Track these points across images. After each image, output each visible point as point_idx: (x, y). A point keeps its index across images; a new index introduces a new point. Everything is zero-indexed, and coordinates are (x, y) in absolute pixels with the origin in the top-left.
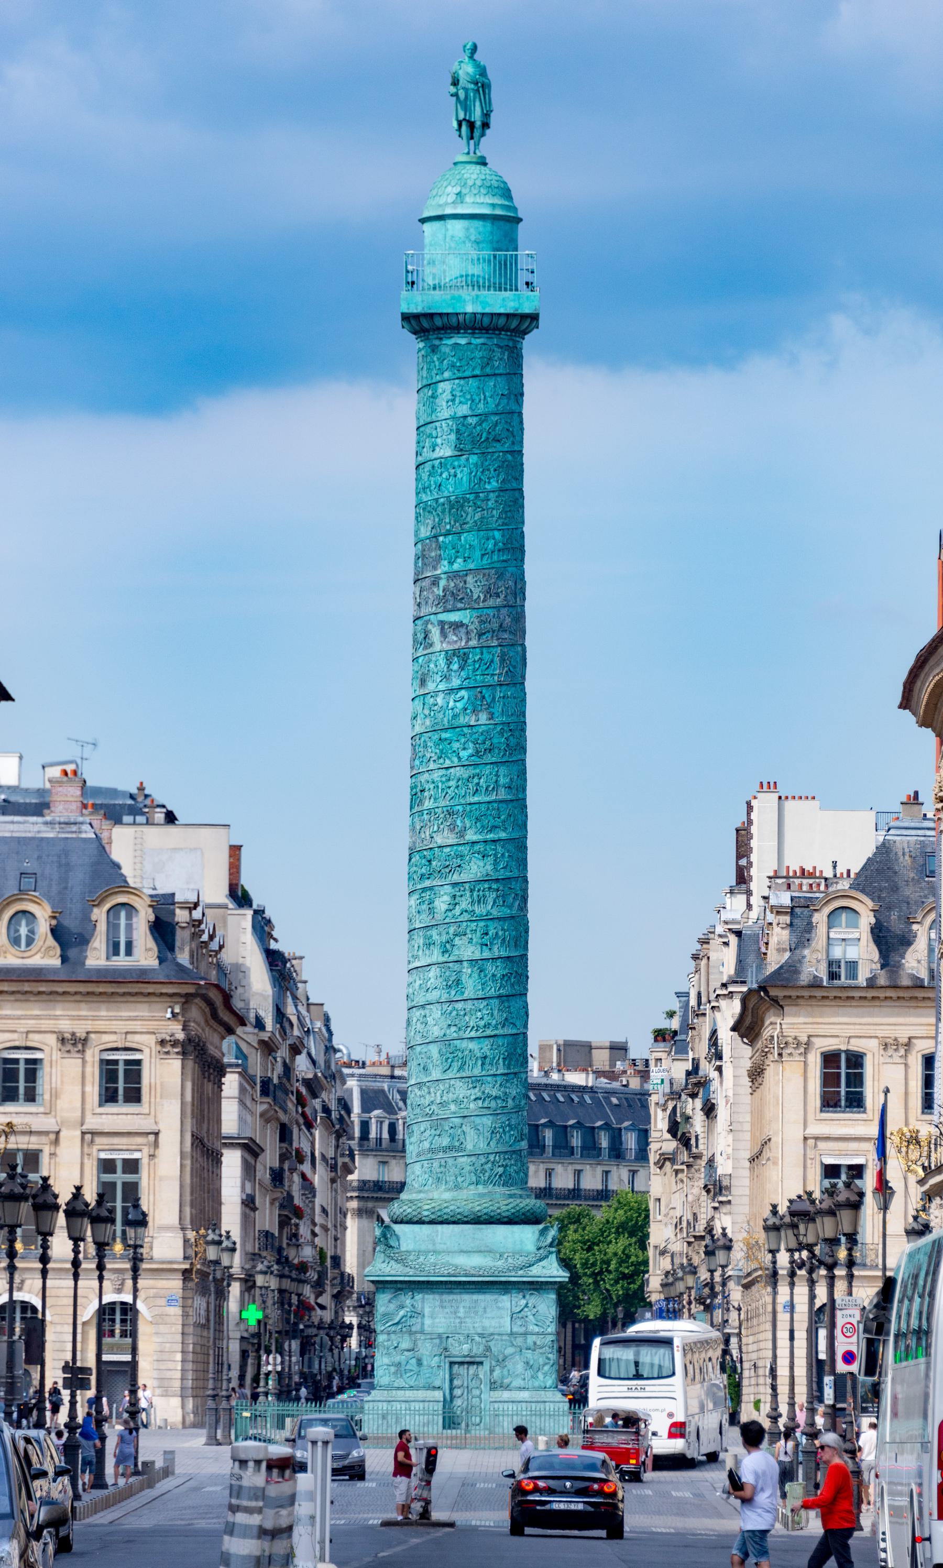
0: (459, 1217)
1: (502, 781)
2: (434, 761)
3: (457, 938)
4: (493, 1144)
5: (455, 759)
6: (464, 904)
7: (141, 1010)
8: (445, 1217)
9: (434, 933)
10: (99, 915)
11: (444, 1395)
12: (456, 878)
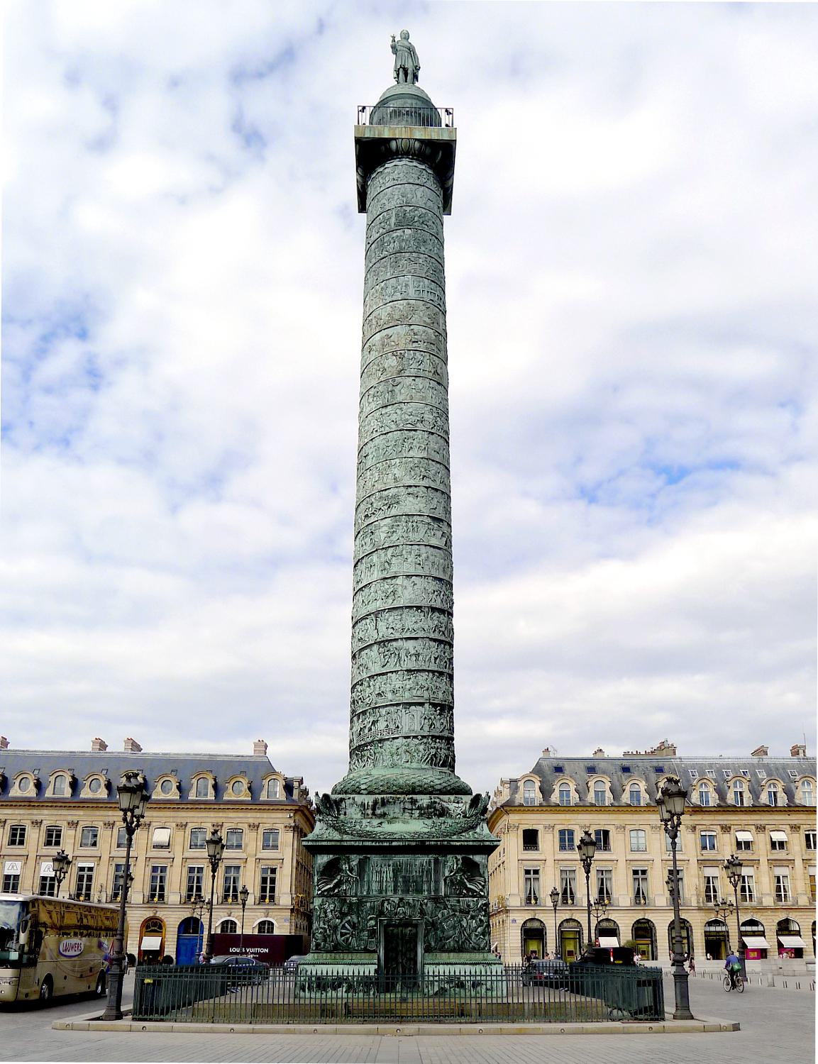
0: (395, 788)
1: (432, 445)
2: (377, 431)
3: (394, 558)
4: (426, 728)
5: (394, 427)
6: (400, 532)
7: (279, 815)
8: (382, 789)
9: (375, 557)
10: (265, 782)
11: (379, 956)
12: (394, 512)
